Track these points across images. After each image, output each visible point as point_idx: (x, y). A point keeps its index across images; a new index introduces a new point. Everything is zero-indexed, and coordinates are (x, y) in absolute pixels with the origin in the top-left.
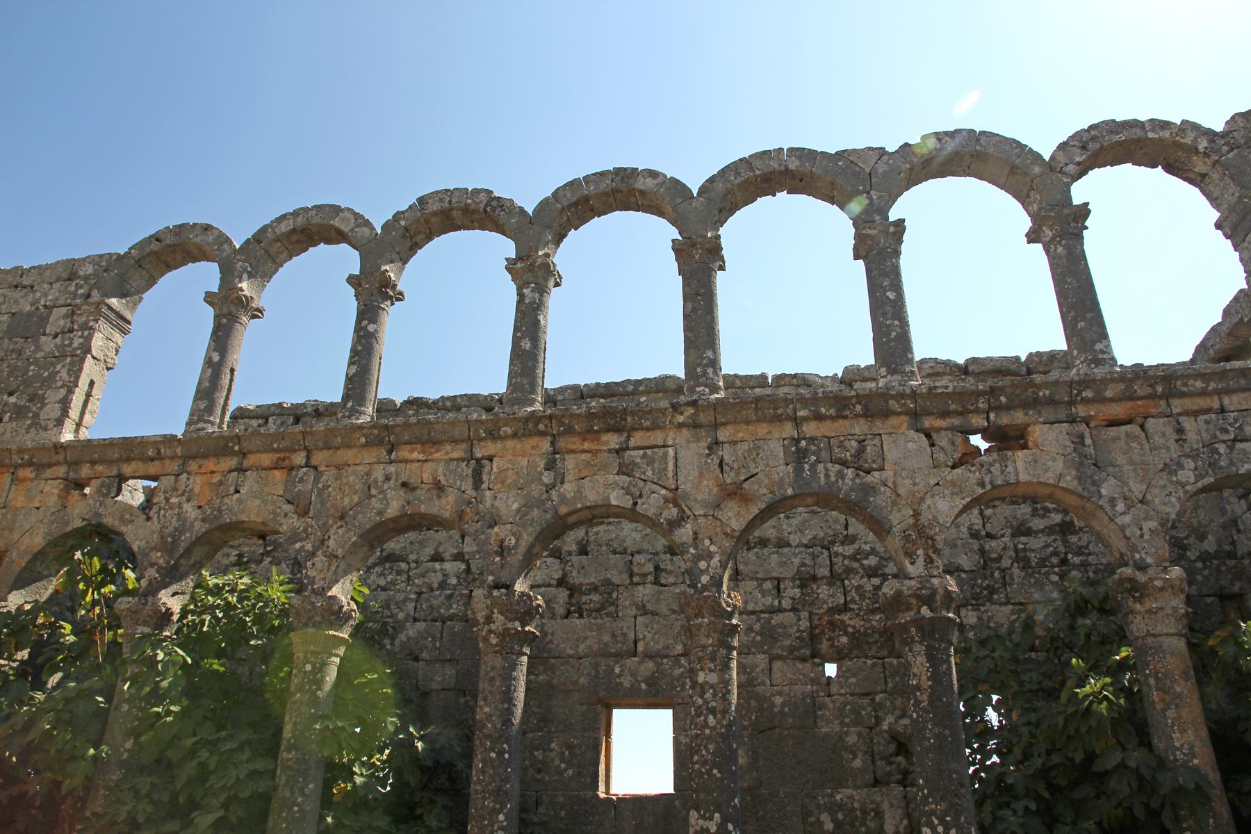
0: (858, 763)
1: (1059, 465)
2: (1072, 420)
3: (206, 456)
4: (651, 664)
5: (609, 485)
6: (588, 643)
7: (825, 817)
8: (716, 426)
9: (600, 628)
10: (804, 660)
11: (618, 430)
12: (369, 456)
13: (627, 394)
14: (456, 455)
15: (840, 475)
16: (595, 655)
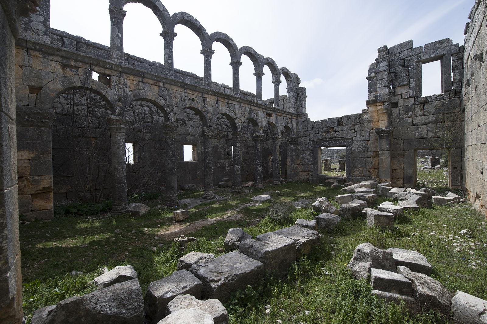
0: (223, 156)
1: (274, 120)
2: (276, 114)
3: (129, 74)
4: (193, 137)
5: (226, 110)
6: (181, 132)
7: (219, 164)
8: (241, 103)
9: (183, 129)
10: (216, 139)
11: (228, 99)
12: (180, 89)
13: (186, 75)
14: (199, 95)
15: (254, 116)
16: (183, 134)
